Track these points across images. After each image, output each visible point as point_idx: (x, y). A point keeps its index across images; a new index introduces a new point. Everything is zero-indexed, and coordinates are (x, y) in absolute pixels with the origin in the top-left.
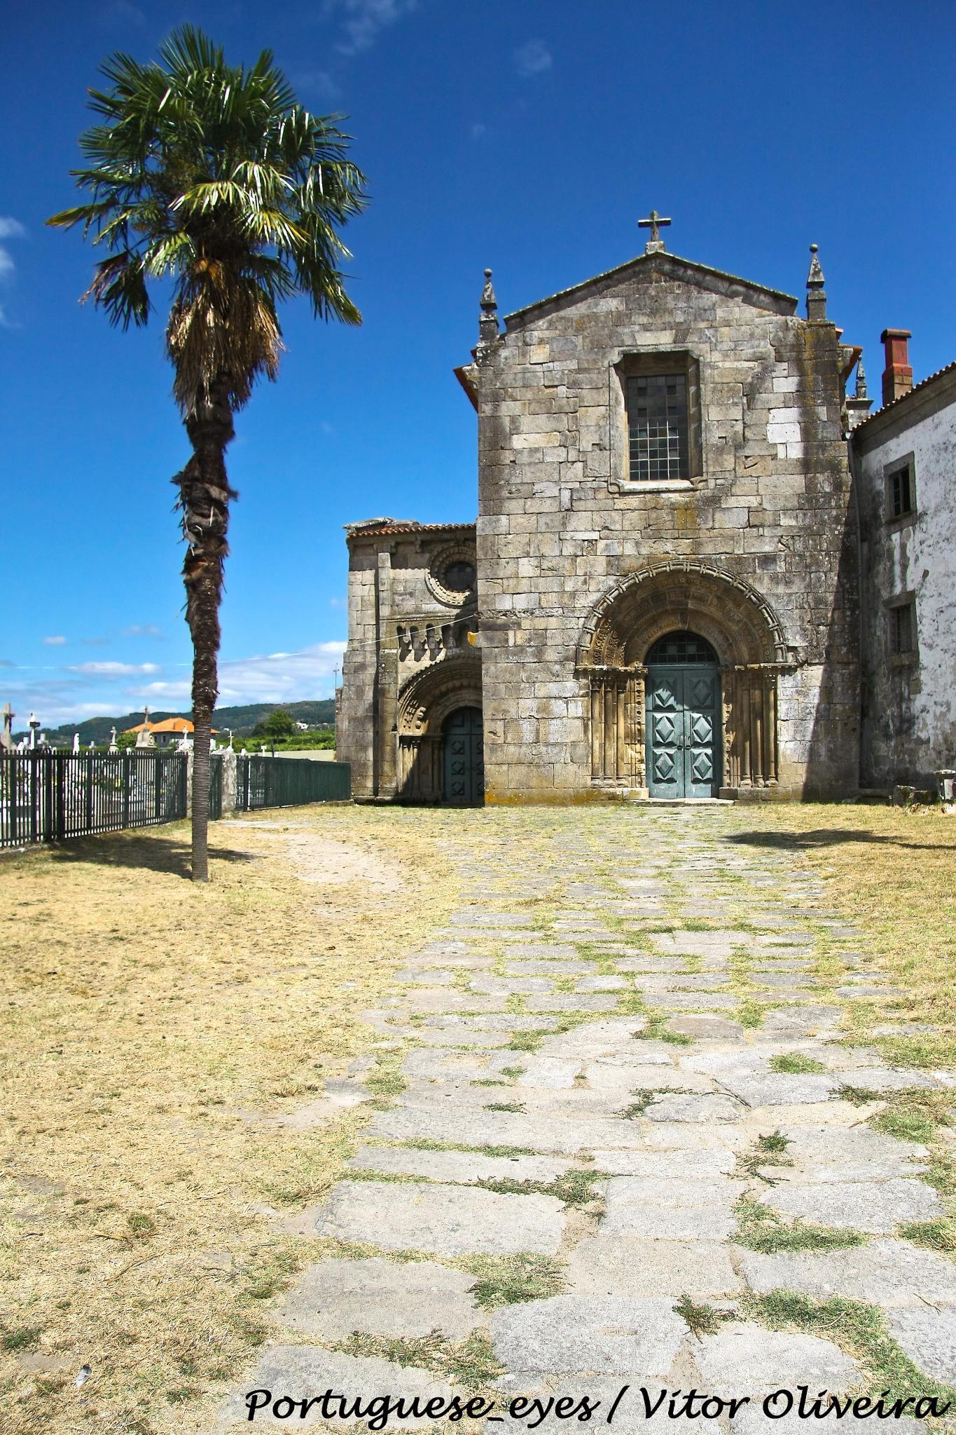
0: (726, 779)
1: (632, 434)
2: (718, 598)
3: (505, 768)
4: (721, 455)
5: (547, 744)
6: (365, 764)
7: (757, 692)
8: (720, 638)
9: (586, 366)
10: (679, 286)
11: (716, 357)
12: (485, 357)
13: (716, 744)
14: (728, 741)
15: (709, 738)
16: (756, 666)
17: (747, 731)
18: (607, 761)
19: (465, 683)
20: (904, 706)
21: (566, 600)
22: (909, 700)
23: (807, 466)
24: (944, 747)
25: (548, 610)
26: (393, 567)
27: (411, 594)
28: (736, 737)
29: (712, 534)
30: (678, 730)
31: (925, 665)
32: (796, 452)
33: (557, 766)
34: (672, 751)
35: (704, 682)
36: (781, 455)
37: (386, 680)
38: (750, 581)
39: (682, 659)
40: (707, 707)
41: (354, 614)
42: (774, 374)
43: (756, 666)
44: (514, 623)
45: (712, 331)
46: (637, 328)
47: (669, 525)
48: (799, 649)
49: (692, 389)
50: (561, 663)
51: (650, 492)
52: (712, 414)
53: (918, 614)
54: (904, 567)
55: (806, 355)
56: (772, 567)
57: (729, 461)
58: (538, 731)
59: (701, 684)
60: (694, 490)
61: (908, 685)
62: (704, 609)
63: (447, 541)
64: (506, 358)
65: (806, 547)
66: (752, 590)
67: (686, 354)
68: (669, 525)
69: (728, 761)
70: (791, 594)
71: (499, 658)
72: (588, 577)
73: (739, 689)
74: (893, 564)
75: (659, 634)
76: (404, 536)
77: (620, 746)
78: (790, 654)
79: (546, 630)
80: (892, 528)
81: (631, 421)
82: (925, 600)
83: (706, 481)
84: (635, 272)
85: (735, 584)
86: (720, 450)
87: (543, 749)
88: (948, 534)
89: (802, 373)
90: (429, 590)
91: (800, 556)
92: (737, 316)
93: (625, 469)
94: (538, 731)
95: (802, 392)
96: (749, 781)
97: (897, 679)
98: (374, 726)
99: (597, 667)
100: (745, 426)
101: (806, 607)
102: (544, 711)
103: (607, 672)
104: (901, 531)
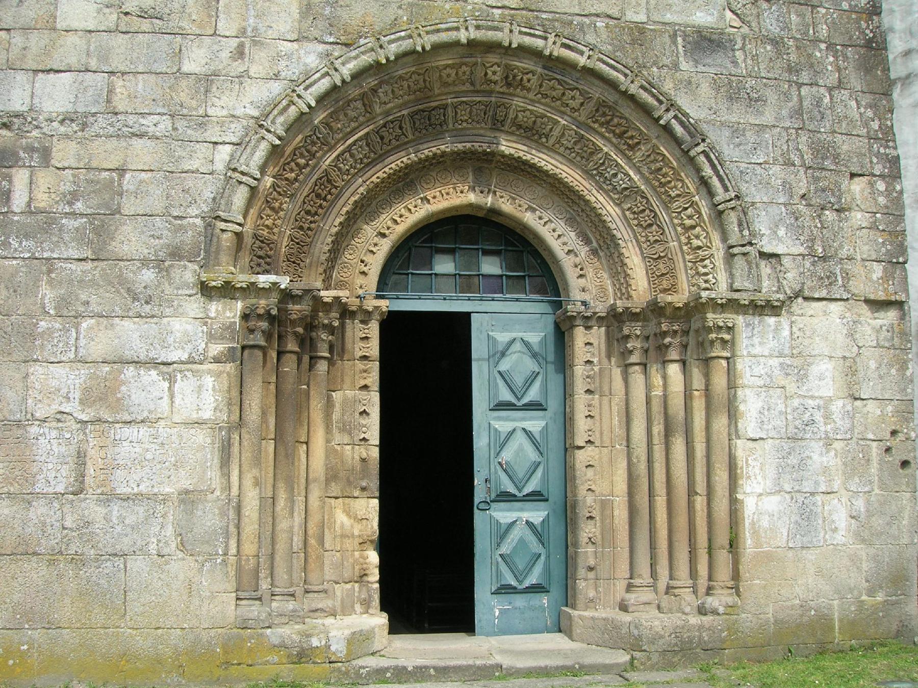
5: (108, 497)
7: (674, 370)
21: (183, 97)
25: (131, 120)
33: (137, 564)
38: (668, 86)
44: (31, 149)
48: (786, 261)
58: (81, 457)
65: (786, 27)
66: (672, 105)
70: (762, 128)
79: (122, 171)
85: (633, 89)
87: (95, 511)
94: (81, 457)
99: (264, 280)
102: (102, 399)
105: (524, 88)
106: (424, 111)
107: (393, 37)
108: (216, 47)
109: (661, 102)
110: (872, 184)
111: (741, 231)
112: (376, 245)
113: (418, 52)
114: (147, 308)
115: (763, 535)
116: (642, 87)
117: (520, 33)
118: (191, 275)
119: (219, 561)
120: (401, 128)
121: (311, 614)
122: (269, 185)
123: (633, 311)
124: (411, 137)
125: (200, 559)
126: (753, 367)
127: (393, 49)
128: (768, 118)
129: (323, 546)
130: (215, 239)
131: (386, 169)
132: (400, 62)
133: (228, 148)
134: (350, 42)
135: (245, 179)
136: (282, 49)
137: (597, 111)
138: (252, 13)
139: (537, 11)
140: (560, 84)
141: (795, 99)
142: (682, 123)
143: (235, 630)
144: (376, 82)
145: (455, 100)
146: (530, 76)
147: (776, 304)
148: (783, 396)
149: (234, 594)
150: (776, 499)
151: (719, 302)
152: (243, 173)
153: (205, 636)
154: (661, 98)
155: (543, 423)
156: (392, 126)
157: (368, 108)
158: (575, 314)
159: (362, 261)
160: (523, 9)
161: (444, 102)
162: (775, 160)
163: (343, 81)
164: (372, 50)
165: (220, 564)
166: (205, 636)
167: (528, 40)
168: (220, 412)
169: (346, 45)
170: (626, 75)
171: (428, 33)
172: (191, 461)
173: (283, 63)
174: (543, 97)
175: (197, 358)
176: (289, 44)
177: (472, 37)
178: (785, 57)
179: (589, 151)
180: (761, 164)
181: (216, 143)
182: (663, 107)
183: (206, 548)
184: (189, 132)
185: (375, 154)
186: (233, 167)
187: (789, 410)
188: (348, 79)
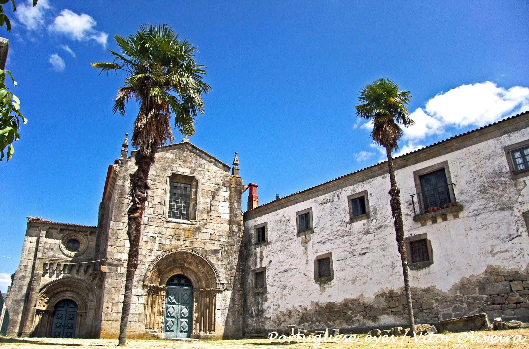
0: (194, 331)
1: (170, 201)
2: (197, 263)
3: (110, 322)
4: (202, 214)
6: (16, 321)
7: (208, 299)
9: (159, 174)
10: (194, 155)
11: (204, 180)
12: (122, 163)
13: (190, 318)
14: (195, 317)
15: (187, 315)
16: (209, 289)
17: (203, 313)
18: (151, 322)
19: (69, 289)
20: (260, 306)
22: (262, 304)
23: (230, 222)
24: (277, 320)
26: (46, 237)
27: (52, 249)
28: (198, 315)
29: (197, 240)
30: (176, 311)
31: (269, 292)
32: (227, 217)
34: (173, 319)
35: (187, 294)
36: (222, 217)
37: (34, 284)
38: (209, 259)
39: (179, 285)
40: (187, 304)
41: (24, 254)
42: (222, 190)
43: (209, 289)
44: (121, 264)
45: (203, 172)
46: (178, 165)
48: (224, 284)
49: (194, 190)
50: (138, 282)
51: (177, 223)
52: (201, 199)
53: (267, 275)
54: (262, 259)
55: (232, 186)
56: (217, 254)
57: (205, 216)
59: (186, 295)
60: (192, 224)
61: (262, 299)
62: (190, 267)
63: (71, 230)
64: (130, 166)
66: (210, 262)
67: (194, 177)
68: (183, 235)
69: (195, 324)
70: (223, 265)
71: (113, 277)
72: (151, 250)
73: (200, 297)
74: (257, 258)
75: (173, 275)
76: (54, 225)
77: (155, 316)
78: (221, 286)
80: (257, 246)
81: (171, 197)
82: (270, 270)
83: (197, 222)
84: (179, 147)
85: (204, 259)
86: (202, 212)
88: (280, 249)
89: (231, 191)
90: (60, 249)
91: (226, 252)
92: (211, 169)
93: (167, 214)
95: (230, 197)
96: (202, 332)
97: (257, 297)
98: (24, 304)
99: (152, 285)
100: (211, 205)
101: (228, 270)
103: (154, 287)
104: (261, 247)
110: (239, 273)
114: (136, 288)
128: (224, 263)
153: (141, 333)
157: (167, 261)
166: (141, 333)
167: (190, 252)
173: (156, 254)
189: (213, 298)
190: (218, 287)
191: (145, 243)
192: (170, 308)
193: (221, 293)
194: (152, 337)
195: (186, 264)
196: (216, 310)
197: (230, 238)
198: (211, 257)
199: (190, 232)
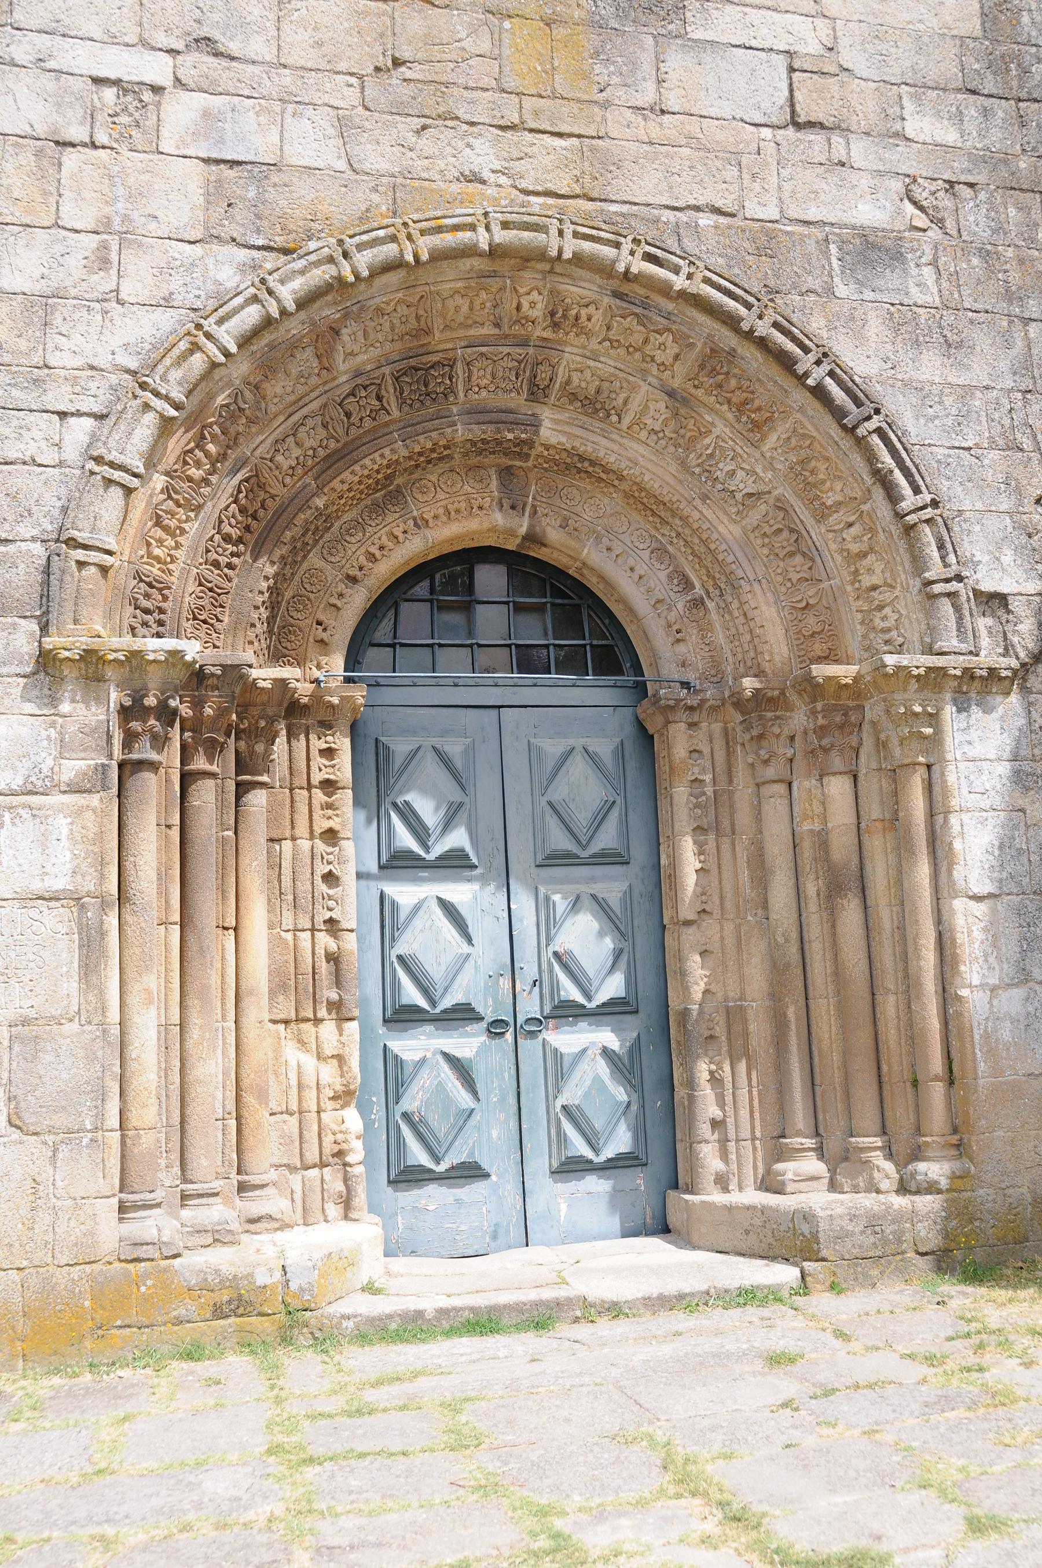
2: (671, 394)
7: (838, 787)
8: (659, 577)
15: (613, 987)
16: (844, 672)
18: (195, 1111)
29: (653, 128)
35: (591, 756)
38: (816, 325)
47: (482, 72)
48: (1014, 604)
56: (892, 279)
69: (715, 1080)
70: (966, 391)
73: (742, 776)
78: (983, 623)
85: (763, 328)
91: (985, 254)
96: (813, 1165)
99: (154, 646)
101: (1027, 444)
105: (583, 332)
106: (417, 369)
107: (365, 238)
108: (58, 249)
109: (806, 350)
111: (943, 558)
112: (341, 595)
113: (407, 264)
115: (1004, 1054)
116: (776, 325)
117: (576, 235)
118: (24, 642)
119: (85, 1141)
120: (379, 398)
121: (252, 1227)
122: (159, 486)
123: (769, 694)
124: (396, 413)
125: (50, 1139)
126: (972, 778)
127: (364, 260)
128: (978, 373)
129: (267, 1104)
130: (68, 578)
131: (357, 468)
132: (378, 282)
133: (88, 423)
134: (292, 245)
135: (117, 475)
136: (177, 256)
137: (702, 367)
138: (120, 191)
139: (601, 200)
140: (641, 323)
141: (1020, 344)
142: (840, 383)
143: (117, 1265)
144: (338, 315)
145: (469, 350)
146: (592, 308)
147: (1004, 673)
148: (1022, 824)
149: (115, 1201)
150: (1018, 994)
151: (915, 672)
152: (112, 465)
153: (61, 1276)
154: (807, 342)
155: (624, 886)
156: (363, 394)
158: (671, 703)
159: (319, 623)
160: (577, 196)
161: (450, 355)
162: (992, 440)
163: (283, 312)
164: (331, 260)
165: (87, 1147)
166: (61, 1276)
167: (587, 246)
168: (83, 876)
169: (286, 252)
170: (749, 306)
171: (423, 232)
172: (32, 965)
174: (612, 347)
175: (39, 783)
176: (187, 247)
177: (497, 239)
178: (1000, 276)
179: (689, 434)
180: (970, 449)
181: (63, 415)
182: (812, 357)
183: (61, 1120)
184: (15, 393)
185: (338, 441)
186: (95, 454)
187: (1033, 847)
188: (291, 306)
189: (896, 774)
190: (950, 641)
191: (27, 158)
192: (418, 922)
193: (988, 710)
194: (219, 1312)
195: (547, 415)
196: (959, 904)
197: (1002, 109)
198: (834, 307)
199: (559, 32)
